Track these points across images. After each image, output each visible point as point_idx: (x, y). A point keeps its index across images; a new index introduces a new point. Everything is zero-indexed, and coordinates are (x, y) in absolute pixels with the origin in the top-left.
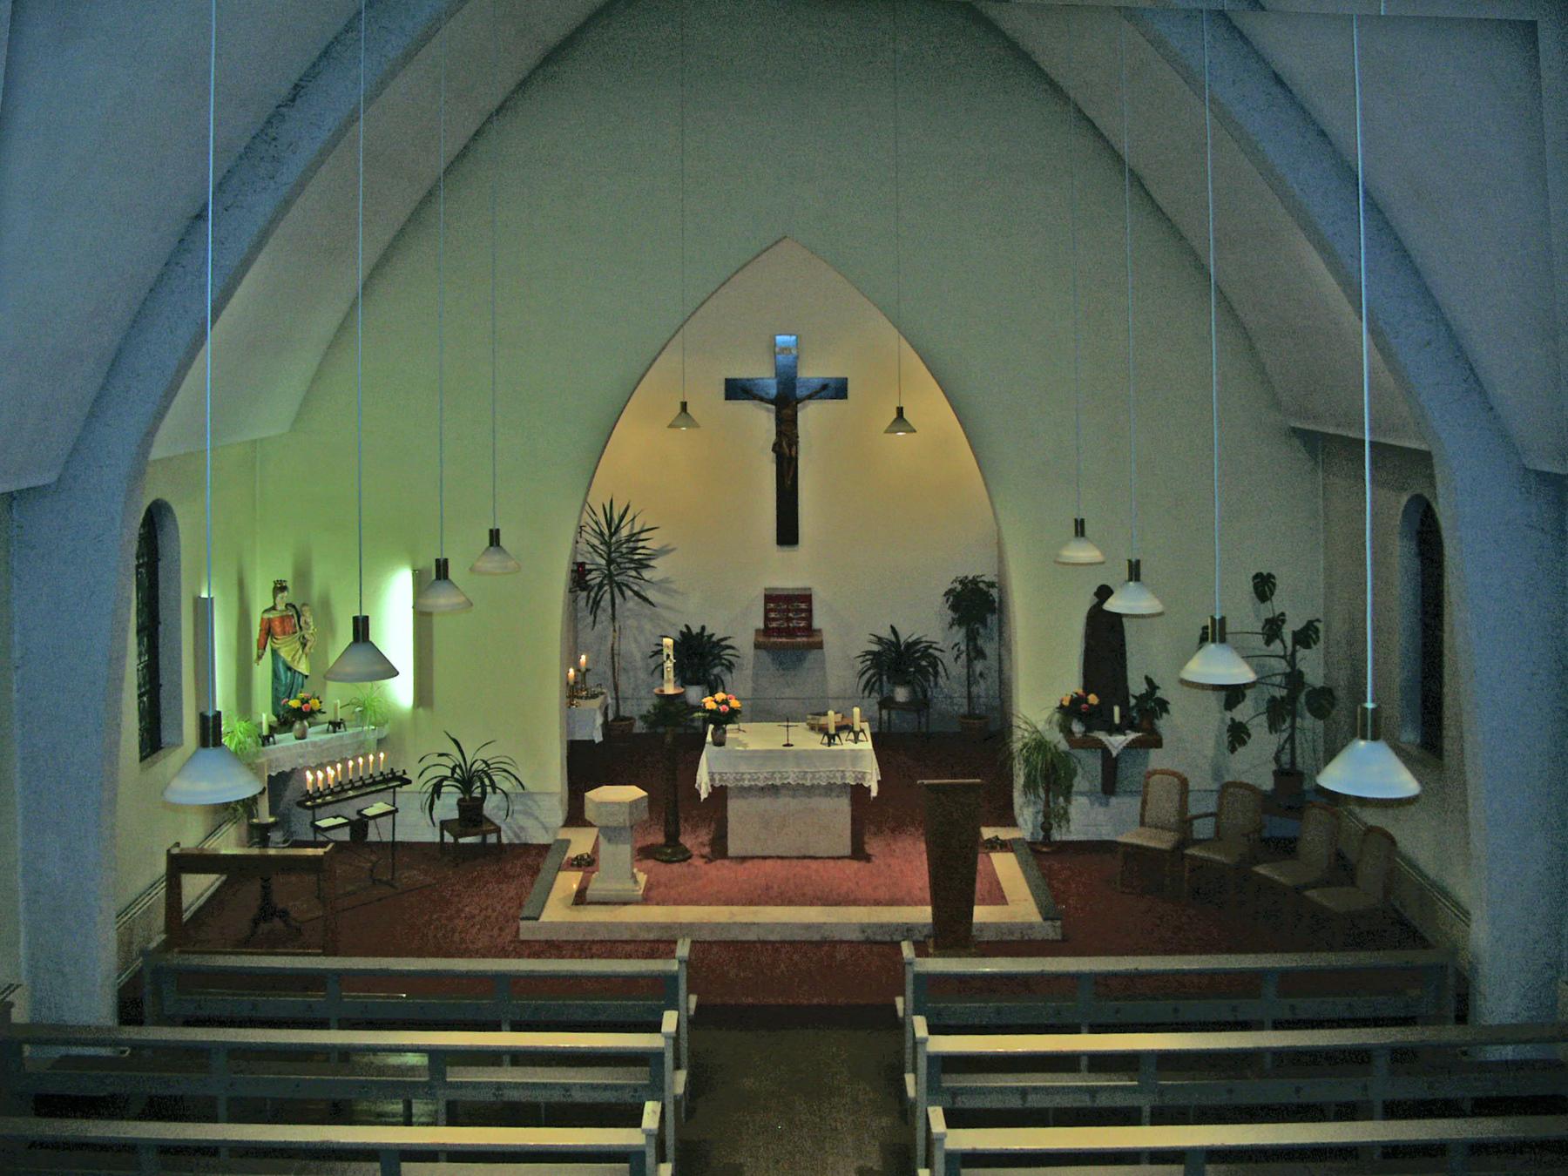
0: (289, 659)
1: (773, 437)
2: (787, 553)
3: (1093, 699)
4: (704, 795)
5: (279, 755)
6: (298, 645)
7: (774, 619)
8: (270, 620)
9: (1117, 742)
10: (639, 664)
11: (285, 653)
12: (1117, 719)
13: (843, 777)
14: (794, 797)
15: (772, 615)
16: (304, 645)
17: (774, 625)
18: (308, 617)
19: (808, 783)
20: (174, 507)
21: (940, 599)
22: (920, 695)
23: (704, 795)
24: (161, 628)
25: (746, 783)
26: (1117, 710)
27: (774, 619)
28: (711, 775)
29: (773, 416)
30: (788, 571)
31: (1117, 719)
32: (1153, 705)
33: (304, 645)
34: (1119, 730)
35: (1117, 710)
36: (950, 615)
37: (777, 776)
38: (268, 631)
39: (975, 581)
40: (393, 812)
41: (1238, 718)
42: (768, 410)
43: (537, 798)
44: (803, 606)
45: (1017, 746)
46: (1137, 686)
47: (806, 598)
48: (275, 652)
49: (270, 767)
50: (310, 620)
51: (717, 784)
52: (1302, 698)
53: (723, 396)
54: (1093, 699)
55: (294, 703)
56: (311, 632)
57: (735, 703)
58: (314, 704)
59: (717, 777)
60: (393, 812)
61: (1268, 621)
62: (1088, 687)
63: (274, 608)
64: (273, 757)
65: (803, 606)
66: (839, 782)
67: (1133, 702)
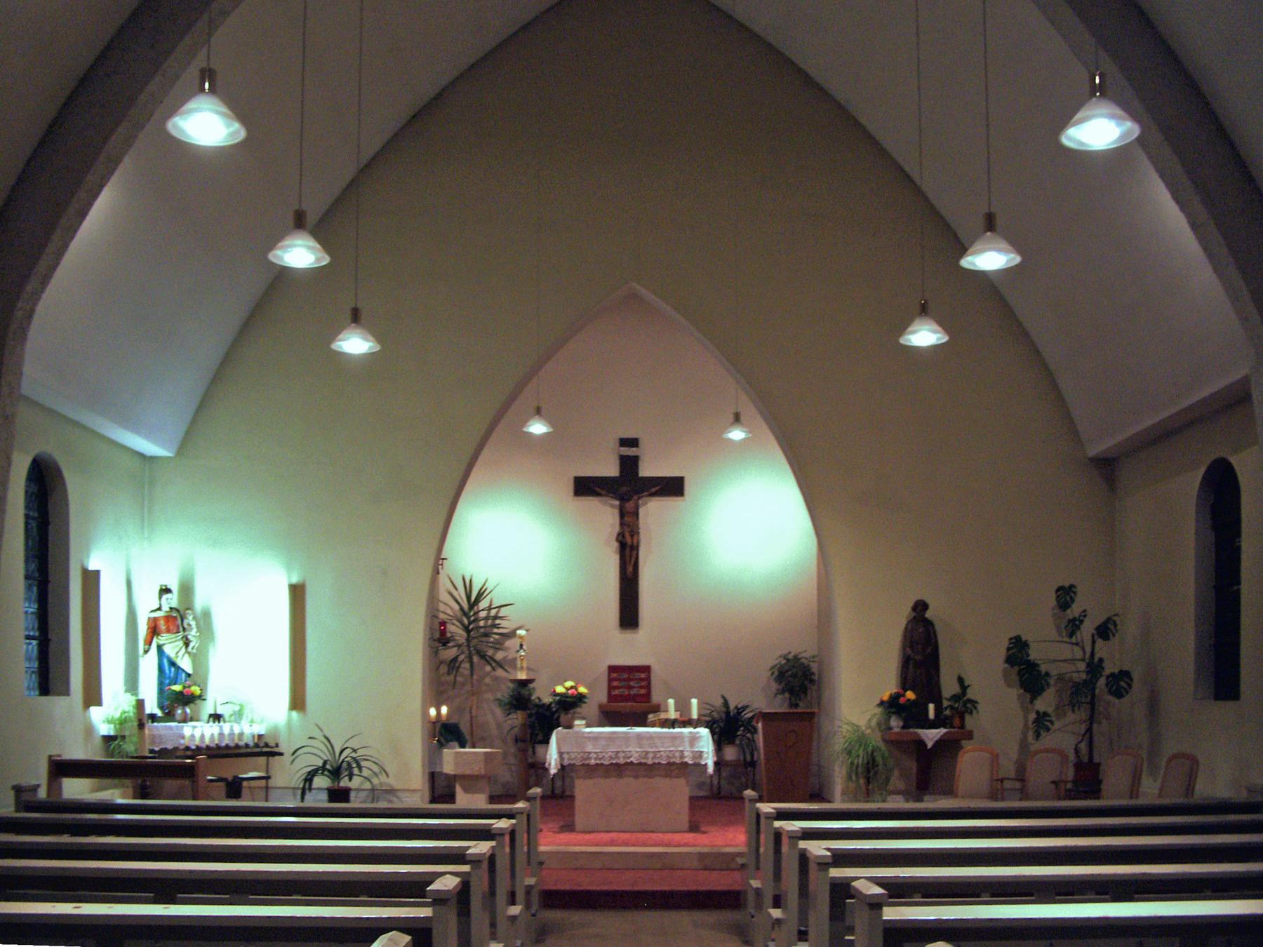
0: (172, 655)
1: (617, 529)
2: (628, 635)
3: (910, 695)
4: (553, 771)
5: (163, 732)
6: (181, 643)
7: (616, 687)
8: (155, 619)
9: (931, 736)
10: (495, 732)
11: (170, 650)
12: (931, 715)
13: (682, 757)
14: (636, 777)
15: (615, 684)
16: (187, 644)
17: (617, 692)
18: (190, 620)
19: (650, 762)
20: (66, 474)
21: (765, 674)
22: (748, 758)
23: (553, 771)
24: (50, 586)
25: (593, 762)
26: (931, 707)
27: (616, 687)
28: (561, 754)
29: (616, 512)
30: (629, 650)
31: (931, 715)
32: (964, 705)
33: (187, 644)
34: (933, 725)
35: (931, 707)
36: (774, 686)
37: (621, 755)
38: (154, 631)
39: (796, 658)
40: (267, 778)
41: (1042, 709)
42: (612, 506)
43: (400, 794)
44: (643, 676)
45: (839, 744)
46: (949, 687)
47: (646, 669)
48: (160, 647)
49: (153, 742)
50: (193, 623)
51: (566, 762)
52: (1102, 682)
53: (572, 493)
54: (910, 695)
55: (177, 688)
56: (193, 634)
57: (582, 690)
58: (196, 690)
59: (566, 756)
60: (267, 778)
61: (1070, 621)
62: (905, 686)
63: (159, 609)
64: (155, 732)
65: (643, 676)
66: (678, 761)
67: (945, 703)
